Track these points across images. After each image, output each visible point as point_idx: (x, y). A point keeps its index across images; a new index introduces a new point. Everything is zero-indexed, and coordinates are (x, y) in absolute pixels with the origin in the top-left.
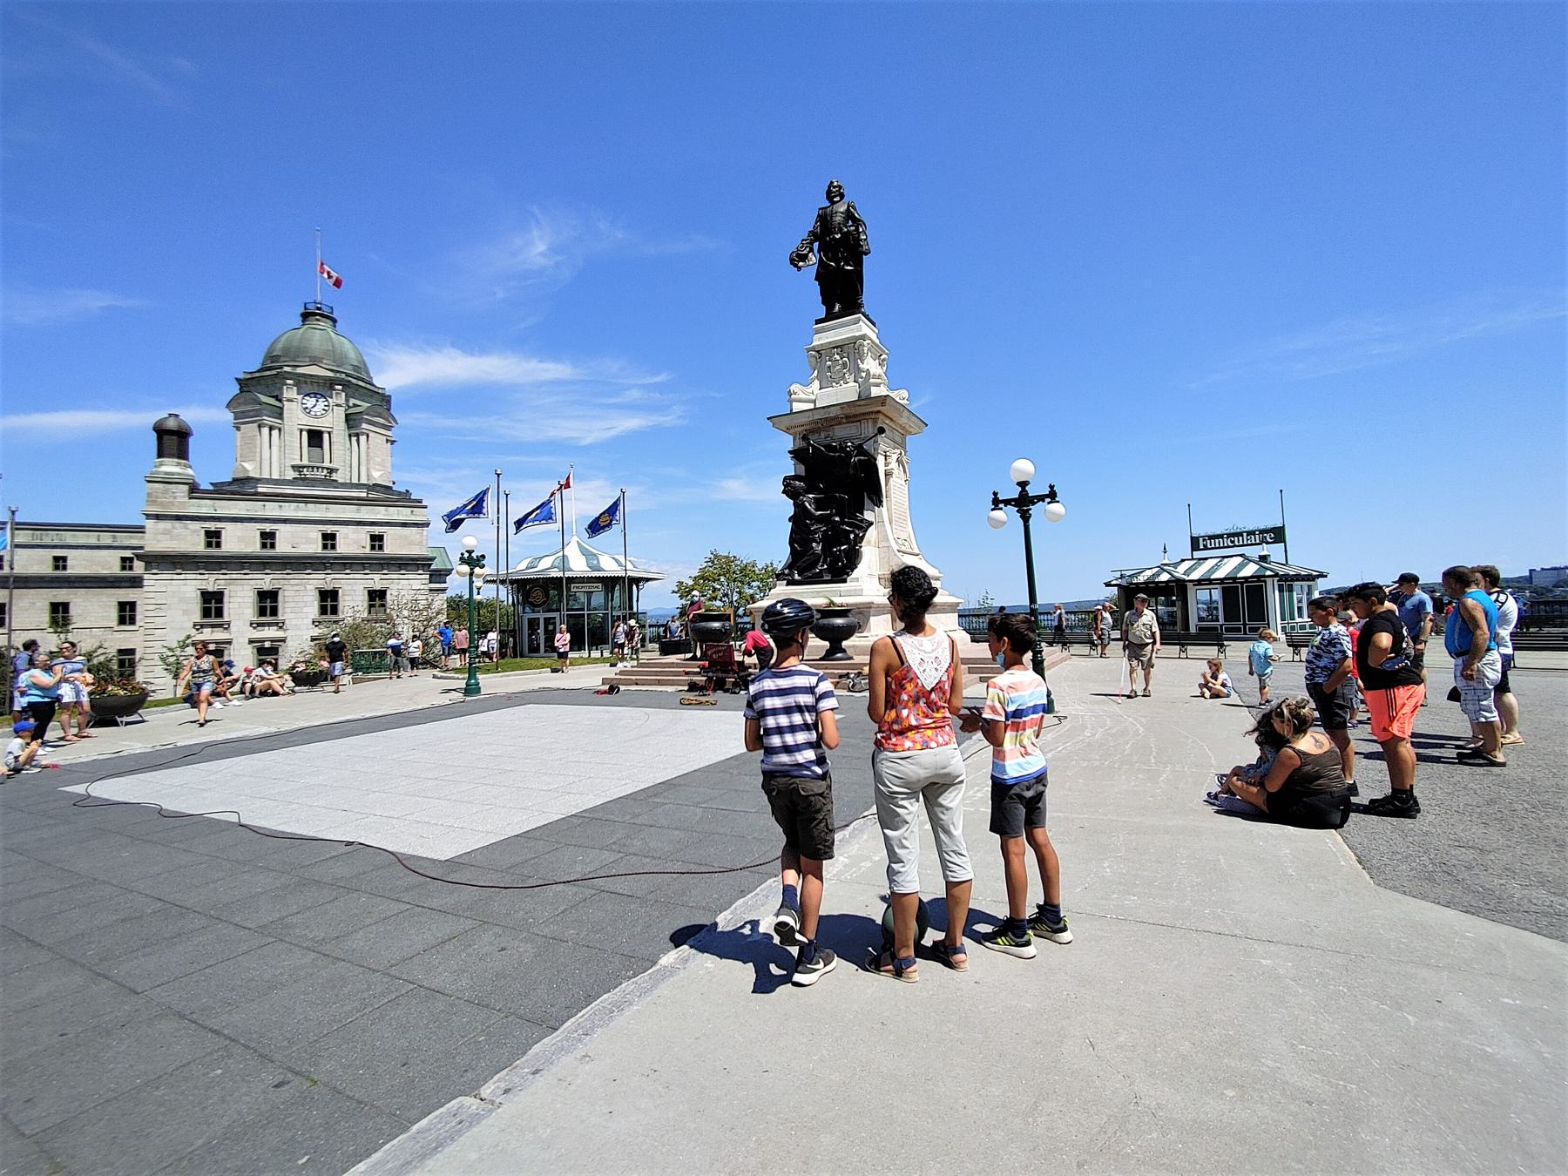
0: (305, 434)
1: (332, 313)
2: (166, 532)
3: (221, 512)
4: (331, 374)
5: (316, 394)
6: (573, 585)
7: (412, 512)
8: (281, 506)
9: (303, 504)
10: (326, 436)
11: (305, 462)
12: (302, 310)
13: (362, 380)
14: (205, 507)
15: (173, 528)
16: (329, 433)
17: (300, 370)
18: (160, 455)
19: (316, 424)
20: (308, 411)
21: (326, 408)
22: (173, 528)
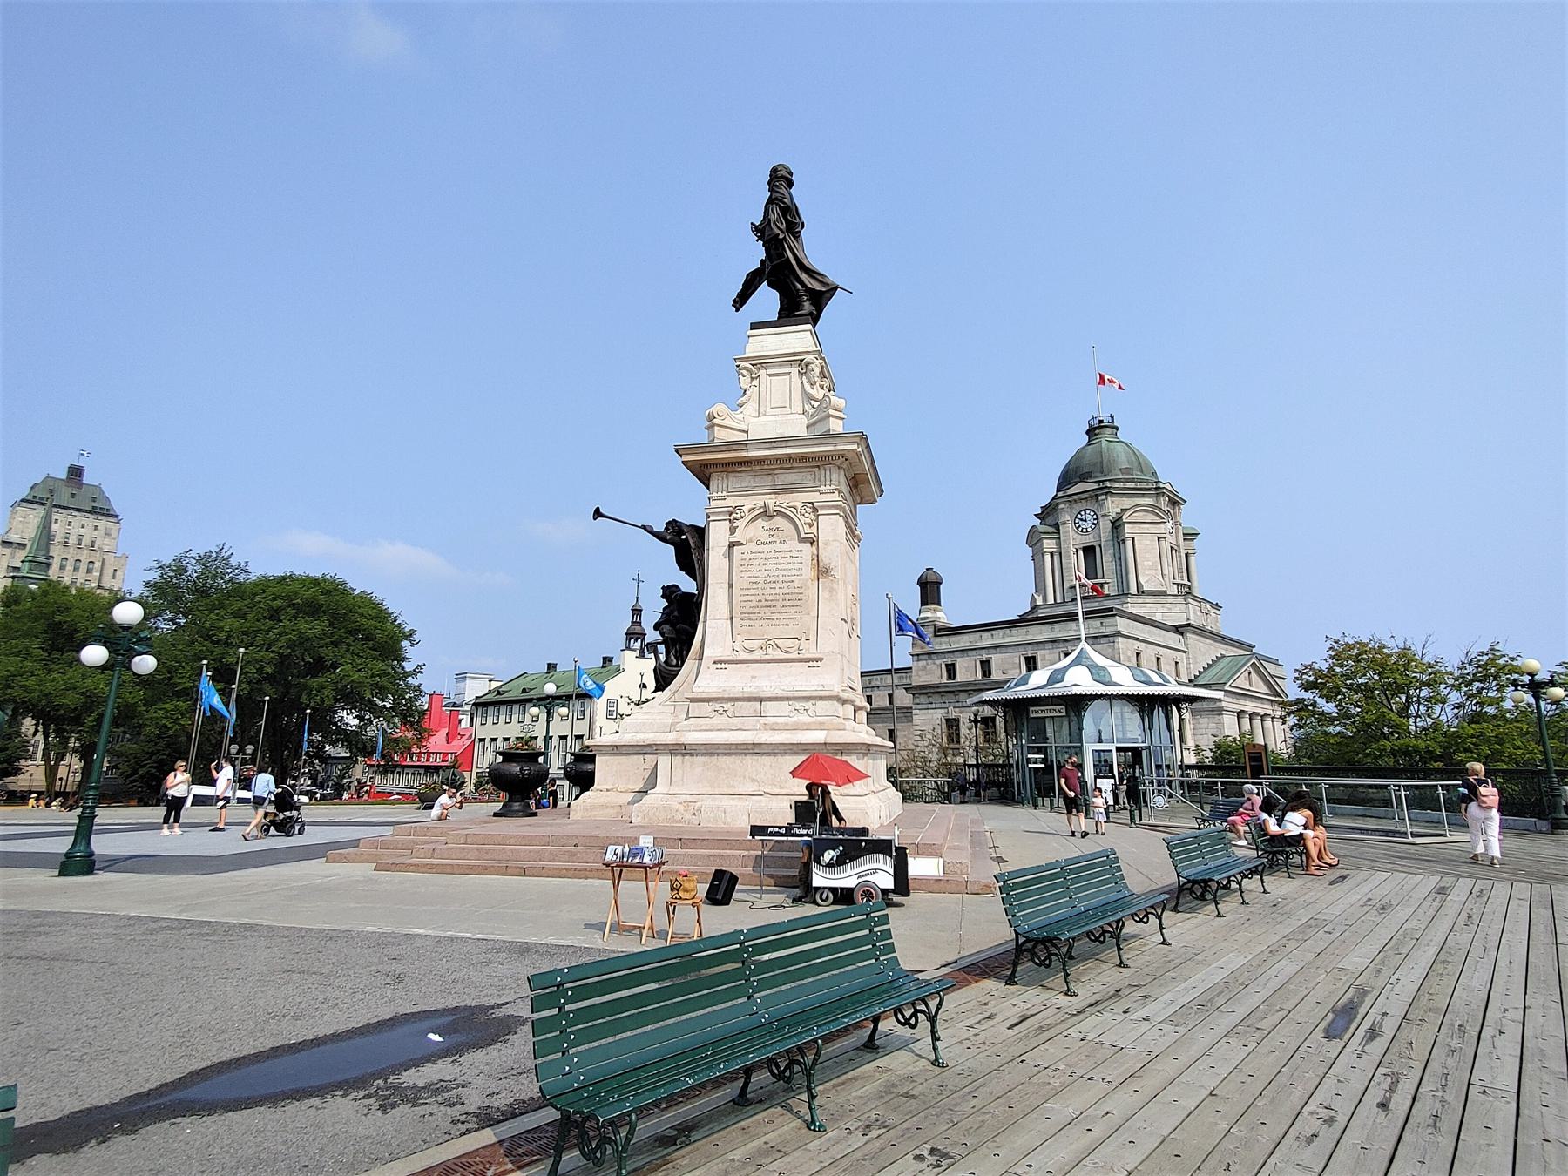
0: (1081, 552)
1: (1113, 422)
2: (924, 668)
3: (955, 647)
4: (1096, 486)
5: (1085, 510)
6: (1031, 709)
7: (1102, 623)
8: (992, 635)
9: (1008, 630)
10: (1098, 549)
12: (1088, 428)
13: (1132, 481)
14: (943, 644)
15: (927, 664)
16: (1100, 546)
17: (1070, 492)
18: (923, 604)
19: (1089, 540)
21: (1095, 522)
22: (927, 664)
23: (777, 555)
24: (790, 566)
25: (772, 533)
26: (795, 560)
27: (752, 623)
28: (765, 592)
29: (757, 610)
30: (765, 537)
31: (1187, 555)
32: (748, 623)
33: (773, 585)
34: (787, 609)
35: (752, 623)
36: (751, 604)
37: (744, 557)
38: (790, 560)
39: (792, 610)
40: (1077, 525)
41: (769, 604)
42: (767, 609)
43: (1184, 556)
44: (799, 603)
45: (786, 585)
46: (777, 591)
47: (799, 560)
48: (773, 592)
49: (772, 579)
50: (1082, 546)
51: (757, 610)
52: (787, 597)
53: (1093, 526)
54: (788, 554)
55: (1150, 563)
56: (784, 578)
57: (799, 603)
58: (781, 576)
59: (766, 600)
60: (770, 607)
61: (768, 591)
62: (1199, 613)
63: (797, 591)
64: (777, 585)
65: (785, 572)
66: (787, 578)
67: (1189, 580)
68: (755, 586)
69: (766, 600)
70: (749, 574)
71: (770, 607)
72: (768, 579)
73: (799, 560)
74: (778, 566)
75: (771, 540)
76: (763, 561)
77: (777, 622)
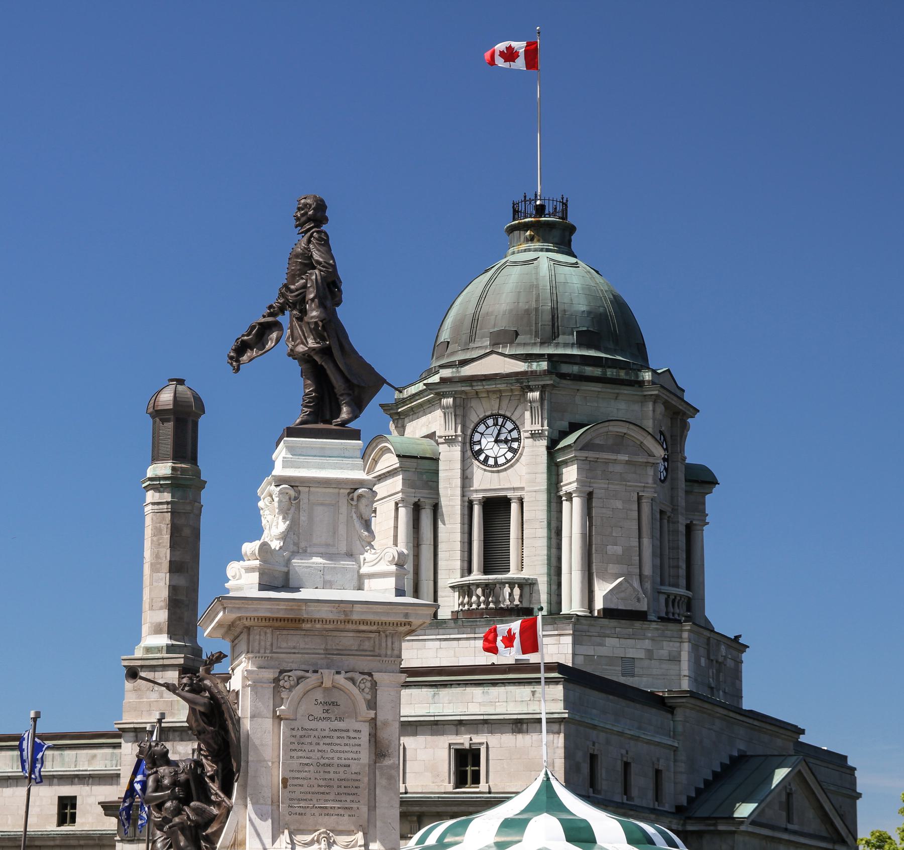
0: (477, 509)
4: (520, 366)
7: (533, 693)
10: (514, 507)
11: (477, 576)
16: (521, 501)
20: (515, 445)
23: (332, 734)
24: (347, 748)
25: (326, 708)
26: (352, 741)
27: (302, 810)
28: (317, 776)
29: (309, 796)
30: (318, 711)
31: (689, 528)
32: (298, 810)
33: (328, 769)
34: (343, 798)
35: (302, 810)
36: (302, 790)
37: (294, 733)
38: (346, 741)
39: (349, 798)
40: (477, 448)
41: (322, 790)
42: (320, 796)
43: (682, 529)
44: (355, 791)
45: (342, 769)
46: (332, 775)
47: (357, 741)
48: (327, 776)
49: (326, 761)
50: (480, 496)
51: (309, 796)
52: (344, 783)
53: (509, 455)
54: (345, 734)
55: (619, 550)
56: (339, 762)
57: (355, 791)
58: (336, 759)
59: (319, 786)
60: (323, 793)
61: (323, 775)
62: (703, 661)
63: (354, 777)
64: (332, 769)
65: (342, 755)
66: (343, 762)
67: (688, 588)
68: (307, 768)
69: (319, 786)
70: (300, 754)
71: (323, 793)
72: (322, 761)
73: (357, 741)
74: (333, 747)
75: (325, 715)
76: (315, 740)
77: (332, 812)
